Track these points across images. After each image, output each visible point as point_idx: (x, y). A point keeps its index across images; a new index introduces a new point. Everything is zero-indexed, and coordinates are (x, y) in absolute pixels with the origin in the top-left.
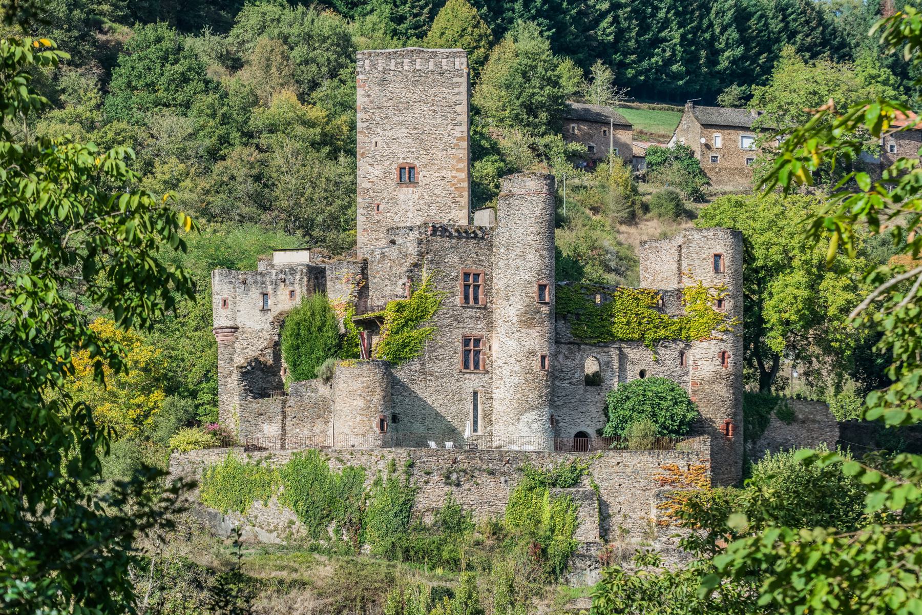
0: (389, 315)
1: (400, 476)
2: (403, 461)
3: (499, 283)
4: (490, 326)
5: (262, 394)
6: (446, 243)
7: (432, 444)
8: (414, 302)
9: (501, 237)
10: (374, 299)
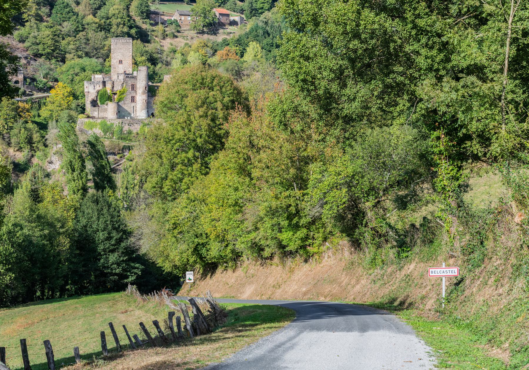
0: (118, 92)
2: (121, 122)
3: (138, 86)
4: (136, 94)
5: (94, 106)
6: (128, 79)
9: (138, 78)
10: (115, 89)
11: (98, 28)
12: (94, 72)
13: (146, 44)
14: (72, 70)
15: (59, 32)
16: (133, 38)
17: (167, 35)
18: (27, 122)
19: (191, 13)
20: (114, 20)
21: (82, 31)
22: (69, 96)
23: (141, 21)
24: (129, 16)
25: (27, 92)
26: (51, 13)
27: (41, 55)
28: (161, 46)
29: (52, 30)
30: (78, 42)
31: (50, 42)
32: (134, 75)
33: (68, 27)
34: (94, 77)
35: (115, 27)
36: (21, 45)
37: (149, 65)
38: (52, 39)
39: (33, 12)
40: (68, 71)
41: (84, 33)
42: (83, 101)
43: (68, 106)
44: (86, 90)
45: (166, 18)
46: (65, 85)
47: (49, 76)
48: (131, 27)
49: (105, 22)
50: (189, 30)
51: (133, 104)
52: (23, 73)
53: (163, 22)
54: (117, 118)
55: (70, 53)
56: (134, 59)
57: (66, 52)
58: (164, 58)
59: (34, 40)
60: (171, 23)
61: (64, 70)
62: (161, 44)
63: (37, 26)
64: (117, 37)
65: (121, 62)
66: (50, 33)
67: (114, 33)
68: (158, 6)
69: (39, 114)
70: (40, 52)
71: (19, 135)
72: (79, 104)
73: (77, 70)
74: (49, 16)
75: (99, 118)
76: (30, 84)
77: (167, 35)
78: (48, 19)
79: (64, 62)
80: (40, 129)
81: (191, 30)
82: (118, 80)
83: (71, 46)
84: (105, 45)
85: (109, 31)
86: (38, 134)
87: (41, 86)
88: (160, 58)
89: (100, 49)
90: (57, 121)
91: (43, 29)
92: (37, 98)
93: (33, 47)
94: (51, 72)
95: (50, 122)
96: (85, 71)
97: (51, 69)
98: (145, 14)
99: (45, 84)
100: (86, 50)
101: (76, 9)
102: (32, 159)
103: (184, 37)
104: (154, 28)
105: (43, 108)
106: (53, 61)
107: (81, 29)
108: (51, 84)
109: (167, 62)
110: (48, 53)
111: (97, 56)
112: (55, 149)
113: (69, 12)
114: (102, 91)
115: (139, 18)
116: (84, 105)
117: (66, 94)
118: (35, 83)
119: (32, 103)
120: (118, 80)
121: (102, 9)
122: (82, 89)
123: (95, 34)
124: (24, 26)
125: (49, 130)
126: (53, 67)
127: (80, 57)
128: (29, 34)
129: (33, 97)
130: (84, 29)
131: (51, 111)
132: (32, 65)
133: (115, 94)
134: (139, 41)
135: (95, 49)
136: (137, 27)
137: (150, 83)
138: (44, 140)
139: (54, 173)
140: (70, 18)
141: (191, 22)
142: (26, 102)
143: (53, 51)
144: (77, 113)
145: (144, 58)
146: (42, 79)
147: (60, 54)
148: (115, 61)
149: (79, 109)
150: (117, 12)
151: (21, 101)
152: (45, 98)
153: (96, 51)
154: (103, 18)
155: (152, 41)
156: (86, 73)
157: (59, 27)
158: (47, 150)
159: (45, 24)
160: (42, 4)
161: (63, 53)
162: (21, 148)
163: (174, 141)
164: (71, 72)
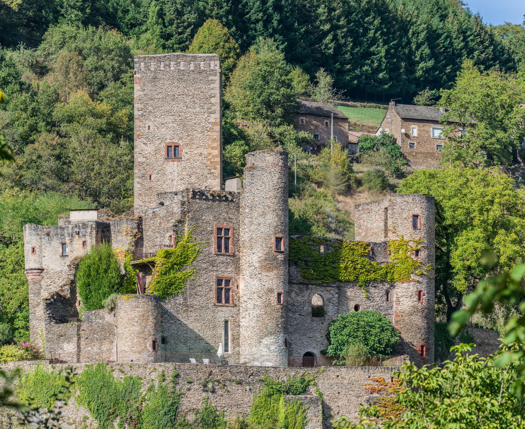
0: (159, 260)
1: (168, 383)
3: (245, 236)
4: (238, 269)
5: (62, 320)
6: (204, 204)
7: (193, 361)
9: (246, 200)
10: (147, 248)
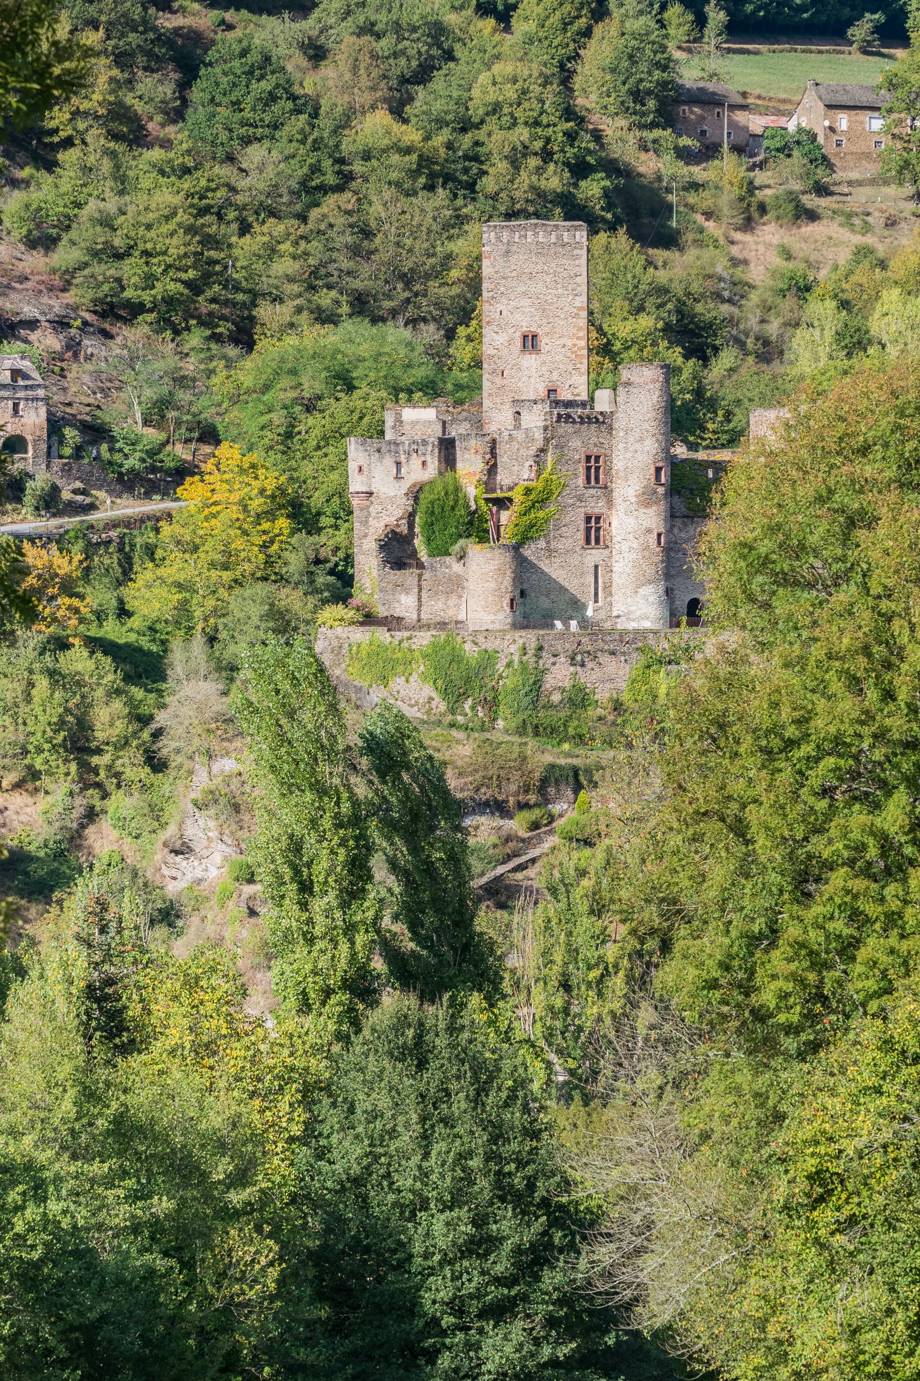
0: (517, 496)
1: (530, 658)
2: (533, 645)
3: (618, 464)
4: (610, 503)
6: (569, 428)
7: (558, 624)
8: (540, 485)
9: (620, 422)
10: (503, 478)
11: (414, 174)
12: (396, 391)
13: (660, 255)
14: (286, 381)
15: (222, 193)
16: (594, 224)
17: (763, 209)
18: (63, 645)
19: (886, 97)
20: (498, 136)
21: (339, 189)
22: (270, 515)
23: (632, 138)
24: (569, 113)
25: (66, 495)
26: (185, 102)
27: (136, 310)
28: (735, 262)
29: (187, 184)
30: (315, 246)
31: (176, 246)
32: (599, 407)
33: (270, 172)
34: (399, 421)
35: (502, 166)
36: (35, 261)
37: (675, 355)
38: (190, 230)
39: (96, 97)
40: (266, 388)
41: (346, 199)
42: (340, 537)
43: (268, 563)
44: (356, 484)
45: (756, 123)
46: (255, 457)
47: (171, 414)
48: (580, 170)
49: (449, 146)
50: (873, 182)
51: (595, 555)
52: (46, 399)
53: (741, 140)
54: (516, 626)
55: (278, 299)
56: (600, 330)
57: (255, 295)
58: (752, 322)
59: (101, 236)
60: (785, 150)
61: (248, 381)
62: (735, 250)
63: (117, 167)
64: (510, 215)
65: (530, 342)
66: (177, 200)
67: (495, 197)
68: (716, 63)
69: (121, 602)
70: (129, 293)
71: (24, 709)
72: (323, 553)
73: (312, 384)
74: (177, 115)
75: (420, 625)
76: (78, 451)
77: (763, 209)
78: (171, 131)
79: (249, 345)
80: (127, 679)
81: (886, 183)
82: (520, 435)
83: (284, 266)
84: (449, 256)
85: (471, 186)
86: (118, 705)
87: (132, 462)
88: (731, 321)
89: (427, 276)
90: (212, 640)
91: (146, 182)
92: (114, 524)
93: (97, 269)
94: (183, 396)
95: (176, 645)
96: (350, 388)
97: (181, 381)
98: (652, 104)
99: (151, 453)
100: (357, 284)
101: (309, 85)
102: (90, 831)
103: (850, 215)
104: (698, 172)
105: (145, 574)
106: (195, 338)
107: (331, 179)
108: (182, 452)
109: (766, 343)
110: (170, 301)
111: (411, 312)
112: (202, 780)
113: (273, 98)
114: (439, 487)
115: (622, 122)
116: (348, 559)
117: (257, 504)
118: (104, 447)
119: (90, 550)
120: (520, 435)
121: (438, 83)
122: (334, 476)
123: (404, 203)
124: (50, 166)
125: (170, 684)
126: (191, 366)
127: (326, 318)
128: (78, 205)
129: (93, 517)
130: (346, 180)
131: (180, 586)
132: (89, 358)
133: (502, 503)
134: (622, 240)
135: (402, 277)
136: (612, 167)
137: (681, 451)
138: (146, 735)
139: (199, 902)
140: (276, 126)
141: (886, 141)
142: (60, 540)
143: (195, 287)
144: (312, 601)
145: (646, 322)
146: (140, 429)
147: (226, 303)
148: (501, 339)
149: (322, 579)
150: (510, 93)
151: (32, 540)
152: (155, 521)
153: (408, 285)
154: (441, 123)
155: (690, 236)
156: (356, 400)
157: (224, 171)
158: (164, 783)
159: (156, 154)
160: (141, 60)
161: (240, 297)
162: (35, 775)
163: (807, 749)
164: (282, 393)
